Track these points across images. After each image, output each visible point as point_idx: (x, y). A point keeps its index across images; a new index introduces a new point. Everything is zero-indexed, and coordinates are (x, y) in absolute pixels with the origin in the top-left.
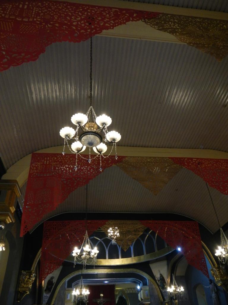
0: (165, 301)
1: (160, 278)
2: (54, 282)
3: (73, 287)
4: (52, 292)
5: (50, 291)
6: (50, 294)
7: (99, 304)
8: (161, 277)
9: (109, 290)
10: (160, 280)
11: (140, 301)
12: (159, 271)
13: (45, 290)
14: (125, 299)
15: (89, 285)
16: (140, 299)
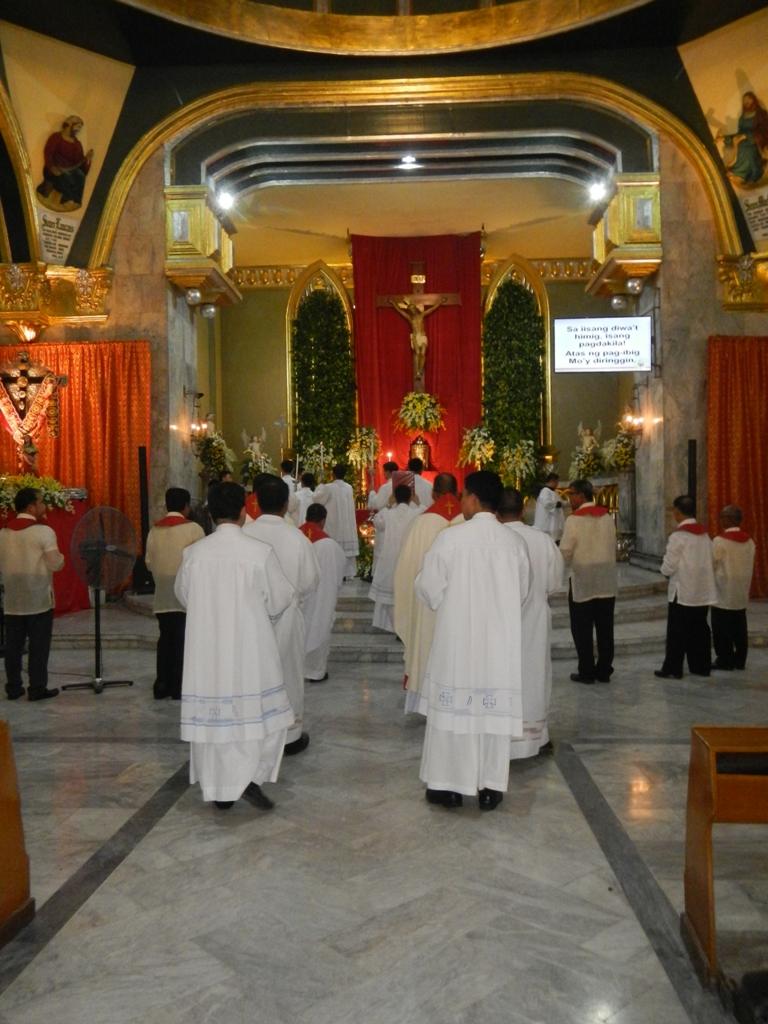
0: (755, 251)
1: (742, 120)
2: (85, 151)
3: (203, 179)
4: (89, 210)
5: (78, 200)
6: (80, 213)
7: (404, 314)
8: (752, 115)
9: (454, 257)
10: (742, 130)
11: (599, 265)
12: (742, 78)
13: (42, 190)
14: (526, 294)
15: (352, 232)
16: (599, 254)
